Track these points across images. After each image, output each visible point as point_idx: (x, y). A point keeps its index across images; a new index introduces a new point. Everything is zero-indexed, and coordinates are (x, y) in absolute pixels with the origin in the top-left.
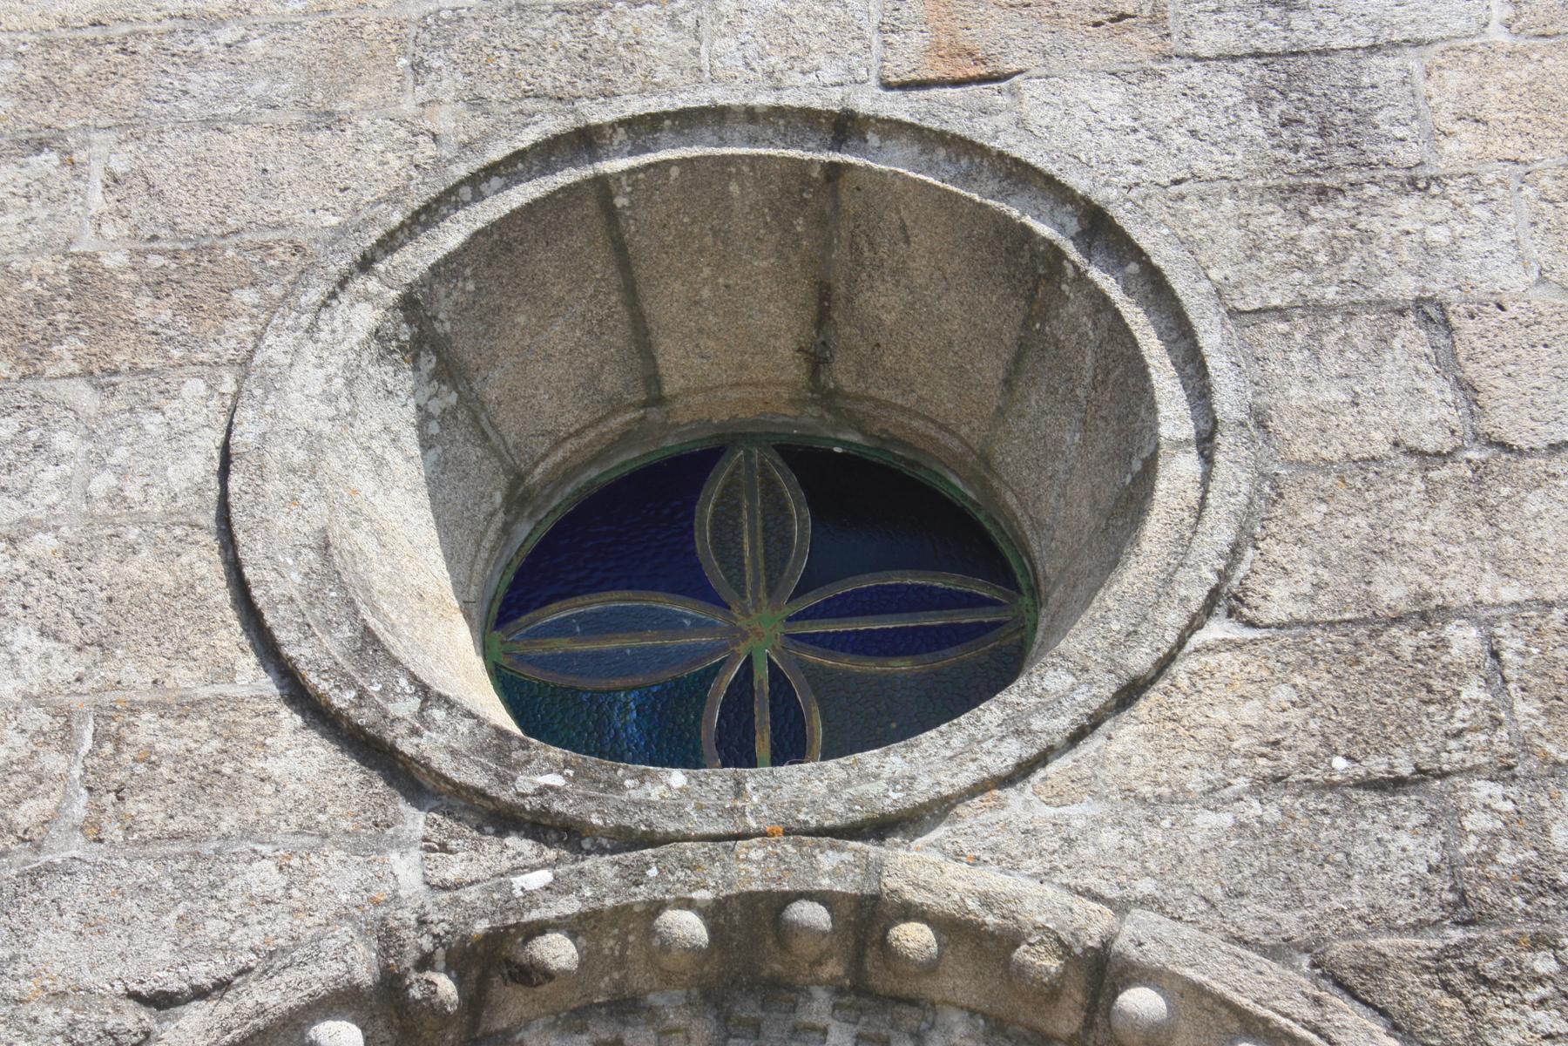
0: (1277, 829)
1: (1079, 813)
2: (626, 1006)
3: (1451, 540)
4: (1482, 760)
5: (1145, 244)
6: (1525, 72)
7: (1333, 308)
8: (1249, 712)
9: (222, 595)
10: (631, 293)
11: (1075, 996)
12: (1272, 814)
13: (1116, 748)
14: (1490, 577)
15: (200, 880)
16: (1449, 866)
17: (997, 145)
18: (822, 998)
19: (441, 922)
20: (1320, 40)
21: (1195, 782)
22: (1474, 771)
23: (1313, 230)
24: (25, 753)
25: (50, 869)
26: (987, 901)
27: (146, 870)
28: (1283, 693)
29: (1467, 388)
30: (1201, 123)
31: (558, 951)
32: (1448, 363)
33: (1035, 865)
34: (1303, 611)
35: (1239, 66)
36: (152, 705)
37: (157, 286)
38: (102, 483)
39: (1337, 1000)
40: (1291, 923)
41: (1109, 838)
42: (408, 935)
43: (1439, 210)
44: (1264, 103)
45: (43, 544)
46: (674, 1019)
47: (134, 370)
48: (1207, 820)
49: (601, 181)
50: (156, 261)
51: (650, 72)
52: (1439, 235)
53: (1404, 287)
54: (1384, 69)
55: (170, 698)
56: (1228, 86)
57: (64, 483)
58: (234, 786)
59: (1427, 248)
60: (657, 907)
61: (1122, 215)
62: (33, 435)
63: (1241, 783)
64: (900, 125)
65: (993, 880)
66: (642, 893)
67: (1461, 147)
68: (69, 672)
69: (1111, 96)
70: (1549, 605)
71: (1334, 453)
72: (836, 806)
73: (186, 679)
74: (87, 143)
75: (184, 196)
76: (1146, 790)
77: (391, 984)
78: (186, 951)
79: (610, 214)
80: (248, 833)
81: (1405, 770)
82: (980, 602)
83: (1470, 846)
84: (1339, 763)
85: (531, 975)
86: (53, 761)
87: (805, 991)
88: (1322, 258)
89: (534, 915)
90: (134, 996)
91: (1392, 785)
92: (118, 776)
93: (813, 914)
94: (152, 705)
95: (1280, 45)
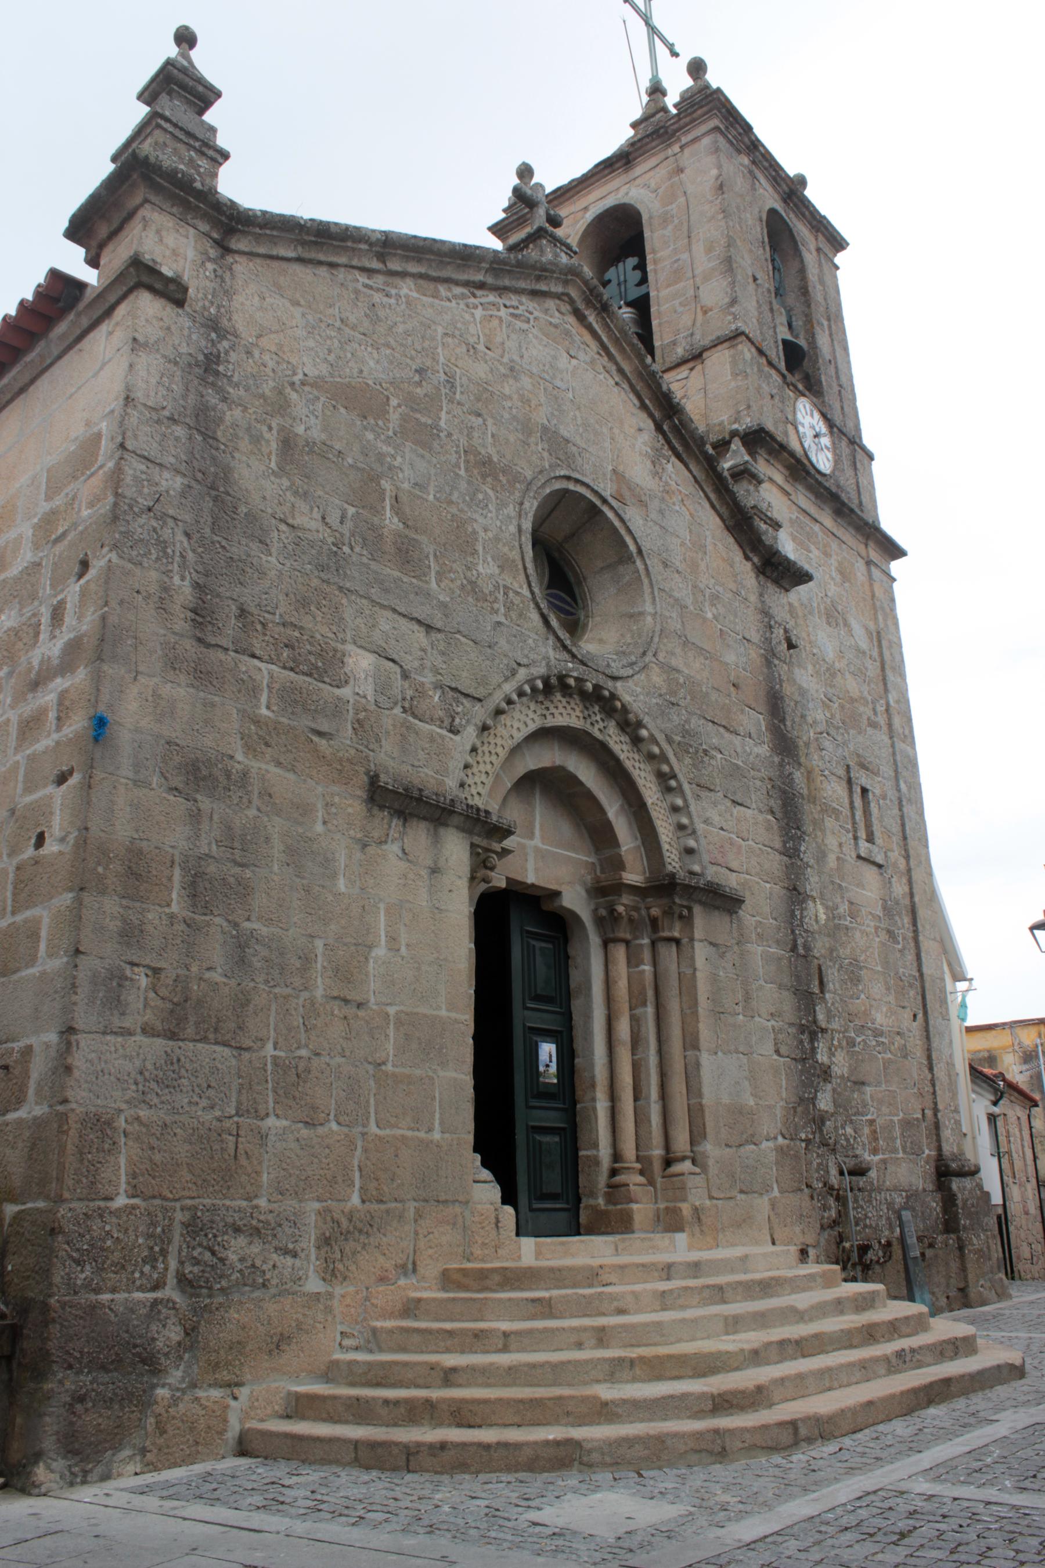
9: (520, 566)
31: (571, 682)
41: (642, 697)
45: (490, 534)
57: (492, 518)
60: (587, 680)
66: (585, 677)
73: (516, 586)
77: (549, 677)
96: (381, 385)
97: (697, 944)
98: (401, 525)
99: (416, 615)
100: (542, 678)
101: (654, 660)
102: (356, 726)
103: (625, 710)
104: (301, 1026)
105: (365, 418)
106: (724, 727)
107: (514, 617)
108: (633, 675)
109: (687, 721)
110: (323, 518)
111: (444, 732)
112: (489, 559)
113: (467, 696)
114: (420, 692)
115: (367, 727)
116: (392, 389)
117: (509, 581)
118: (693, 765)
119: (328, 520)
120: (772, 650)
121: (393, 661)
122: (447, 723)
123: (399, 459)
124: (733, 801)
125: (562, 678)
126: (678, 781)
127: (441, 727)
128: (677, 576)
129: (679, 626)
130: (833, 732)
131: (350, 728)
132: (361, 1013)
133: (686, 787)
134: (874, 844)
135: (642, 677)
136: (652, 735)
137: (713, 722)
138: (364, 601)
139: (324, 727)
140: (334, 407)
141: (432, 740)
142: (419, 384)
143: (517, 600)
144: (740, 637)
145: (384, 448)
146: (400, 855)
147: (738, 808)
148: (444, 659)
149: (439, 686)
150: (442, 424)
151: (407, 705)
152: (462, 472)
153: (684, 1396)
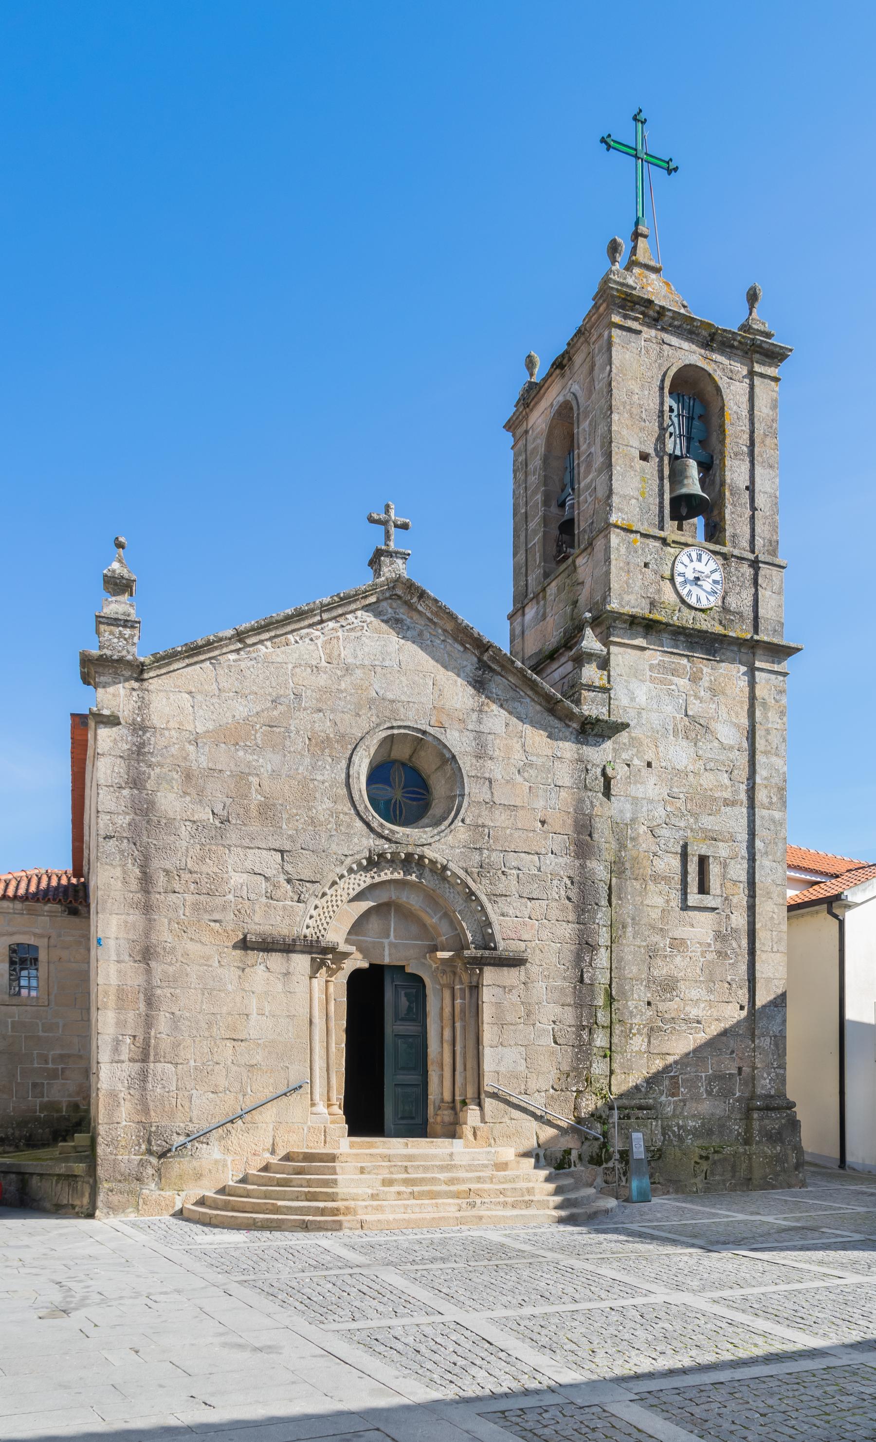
1: (444, 847)
19: (377, 850)
31: (389, 856)
32: (491, 788)
37: (338, 742)
38: (333, 775)
45: (327, 784)
48: (458, 851)
53: (487, 775)
54: (490, 737)
56: (471, 735)
65: (436, 855)
67: (497, 753)
68: (332, 805)
77: (370, 857)
78: (349, 849)
82: (424, 795)
86: (331, 819)
93: (417, 857)
98: (263, 799)
101: (461, 824)
102: (236, 912)
107: (343, 829)
109: (489, 857)
112: (326, 799)
114: (276, 886)
117: (339, 807)
120: (586, 786)
122: (296, 898)
124: (529, 899)
125: (381, 856)
128: (489, 762)
129: (489, 796)
130: (674, 821)
133: (484, 898)
134: (708, 894)
135: (450, 838)
136: (453, 873)
138: (239, 849)
139: (217, 916)
141: (284, 908)
144: (553, 786)
147: (533, 902)
149: (289, 881)
151: (268, 895)
152: (306, 753)
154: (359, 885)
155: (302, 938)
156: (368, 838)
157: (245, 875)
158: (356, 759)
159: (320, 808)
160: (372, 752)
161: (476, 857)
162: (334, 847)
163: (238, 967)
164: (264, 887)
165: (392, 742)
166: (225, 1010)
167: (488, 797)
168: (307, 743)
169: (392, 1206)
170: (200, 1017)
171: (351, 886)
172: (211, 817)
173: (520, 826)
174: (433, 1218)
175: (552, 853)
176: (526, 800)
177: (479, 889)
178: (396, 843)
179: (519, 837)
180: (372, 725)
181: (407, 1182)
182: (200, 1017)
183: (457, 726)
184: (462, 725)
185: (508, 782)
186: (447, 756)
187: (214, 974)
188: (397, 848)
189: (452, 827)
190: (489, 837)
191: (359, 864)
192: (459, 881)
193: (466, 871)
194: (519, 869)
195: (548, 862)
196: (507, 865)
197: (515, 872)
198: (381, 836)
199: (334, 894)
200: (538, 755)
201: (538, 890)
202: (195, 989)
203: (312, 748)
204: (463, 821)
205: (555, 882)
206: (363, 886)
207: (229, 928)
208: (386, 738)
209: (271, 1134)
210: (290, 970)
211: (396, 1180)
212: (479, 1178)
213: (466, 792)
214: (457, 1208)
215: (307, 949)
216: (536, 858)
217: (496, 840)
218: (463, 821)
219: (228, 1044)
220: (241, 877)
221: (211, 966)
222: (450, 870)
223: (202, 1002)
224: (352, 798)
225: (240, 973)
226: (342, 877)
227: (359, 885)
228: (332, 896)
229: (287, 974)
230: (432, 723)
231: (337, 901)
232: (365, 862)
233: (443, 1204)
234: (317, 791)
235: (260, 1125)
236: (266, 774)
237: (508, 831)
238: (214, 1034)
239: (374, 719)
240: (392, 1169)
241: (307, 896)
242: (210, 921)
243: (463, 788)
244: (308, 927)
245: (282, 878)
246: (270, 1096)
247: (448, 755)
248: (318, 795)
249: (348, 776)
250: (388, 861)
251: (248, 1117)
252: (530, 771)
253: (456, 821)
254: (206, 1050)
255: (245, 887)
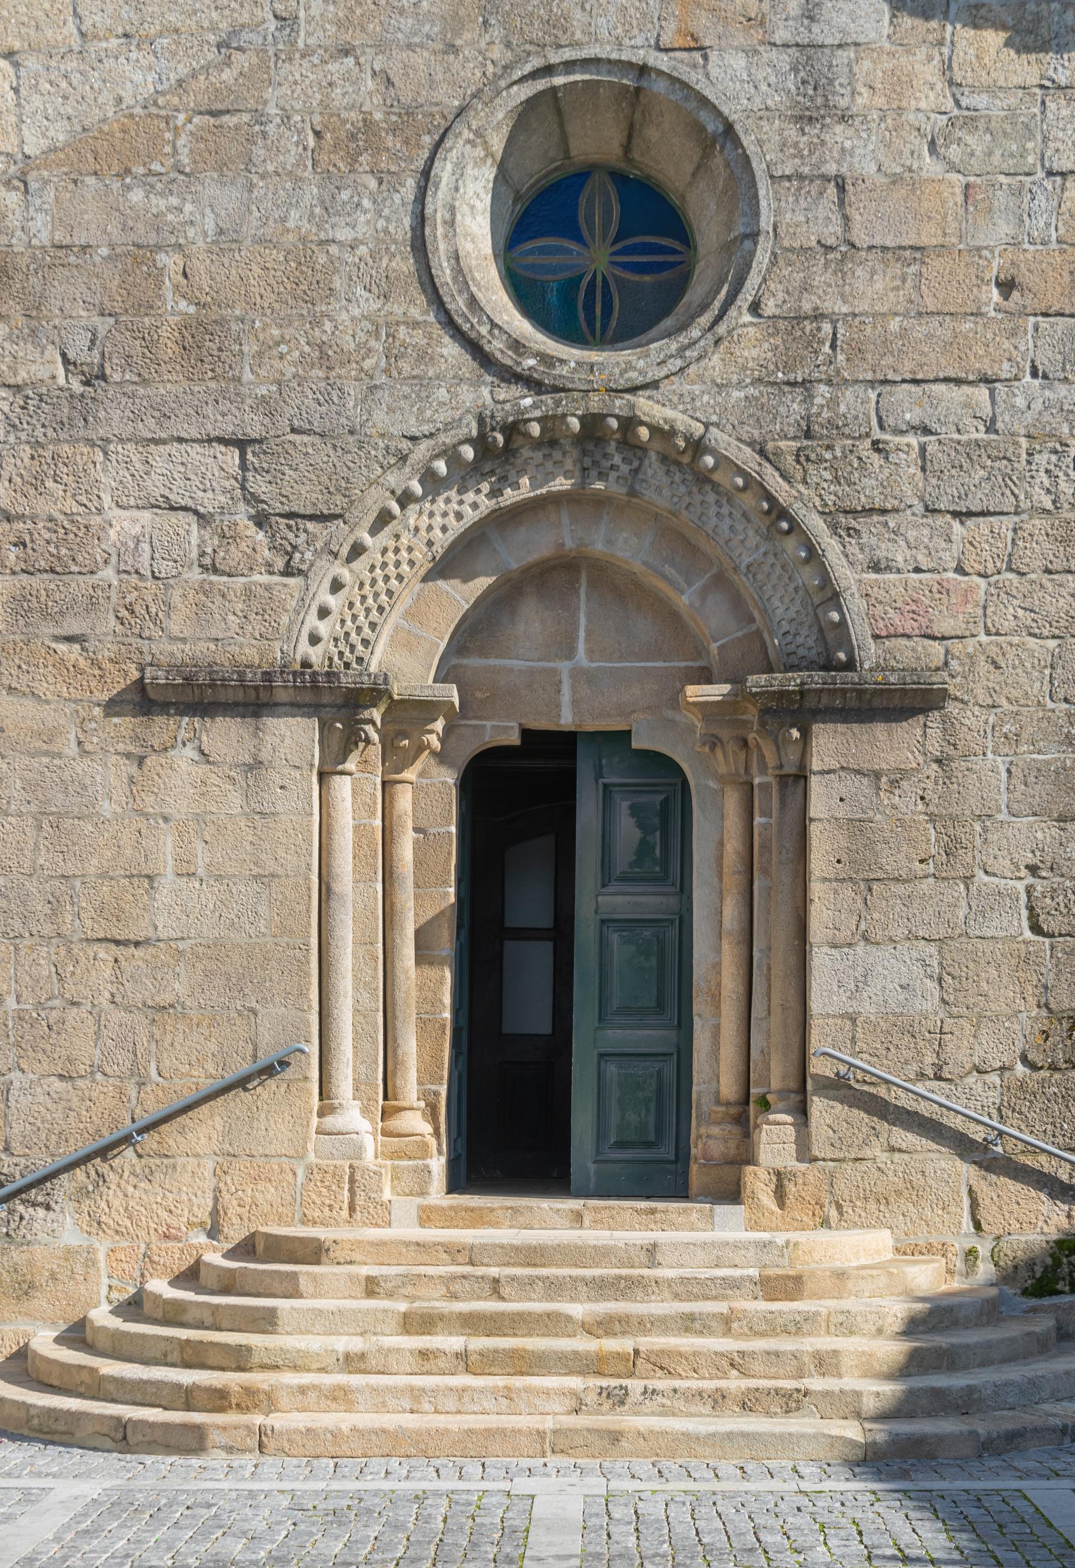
0: (756, 399)
1: (697, 388)
2: (553, 443)
3: (830, 286)
4: (823, 377)
5: (745, 144)
6: (888, 65)
7: (806, 177)
8: (755, 353)
10: (562, 125)
11: (690, 453)
12: (757, 393)
13: (711, 364)
14: (839, 302)
15: (423, 394)
16: (808, 418)
17: (698, 87)
18: (613, 444)
20: (820, 40)
21: (735, 378)
22: (820, 381)
23: (805, 138)
24: (364, 340)
25: (376, 387)
26: (666, 421)
27: (406, 389)
28: (766, 346)
29: (846, 218)
30: (772, 79)
31: (535, 429)
33: (681, 407)
34: (777, 312)
35: (789, 51)
36: (404, 323)
38: (381, 223)
39: (768, 465)
40: (756, 434)
41: (706, 398)
42: (488, 420)
43: (850, 132)
44: (795, 69)
45: (363, 250)
46: (567, 448)
47: (389, 172)
49: (553, 90)
50: (394, 118)
51: (573, 34)
52: (848, 144)
53: (831, 169)
55: (410, 320)
56: (784, 60)
57: (368, 222)
58: (432, 359)
59: (843, 149)
60: (564, 416)
61: (738, 127)
62: (356, 199)
63: (748, 381)
64: (663, 73)
68: (376, 307)
69: (738, 62)
70: (855, 315)
71: (796, 245)
72: (622, 381)
74: (364, 53)
75: (402, 86)
76: (719, 381)
78: (420, 421)
79: (556, 99)
80: (438, 378)
81: (800, 379)
83: (814, 410)
84: (780, 375)
85: (527, 435)
86: (372, 343)
87: (608, 442)
88: (806, 152)
89: (527, 416)
90: (404, 436)
91: (793, 384)
92: (395, 351)
94: (404, 323)
95: (806, 41)
96: (156, 104)
97: (814, 780)
98: (192, 309)
99: (214, 434)
100: (468, 441)
101: (747, 318)
102: (124, 613)
103: (663, 433)
104: (54, 976)
105: (128, 171)
106: (947, 380)
108: (682, 369)
110: (64, 355)
111: (276, 579)
112: (360, 291)
113: (311, 518)
115: (137, 608)
116: (176, 100)
118: (837, 480)
119: (71, 355)
121: (185, 509)
122: (280, 563)
123: (188, 207)
125: (513, 429)
126: (791, 520)
127: (271, 573)
128: (839, 129)
131: (111, 616)
132: (139, 953)
133: (816, 525)
136: (723, 461)
137: (915, 382)
139: (73, 626)
140: (75, 182)
141: (248, 593)
142: (228, 62)
143: (418, 338)
144: (1040, 174)
145: (162, 203)
146: (196, 758)
147: (970, 522)
148: (268, 477)
149: (261, 520)
150: (271, 109)
151: (207, 561)
152: (308, 173)
153: (159, 1384)
154: (459, 516)
155: (297, 667)
156: (477, 384)
157: (146, 515)
158: (444, 171)
159: (344, 316)
160: (498, 143)
161: (794, 407)
162: (380, 416)
163: (128, 755)
164: (194, 540)
165: (559, 112)
166: (92, 866)
167: (832, 232)
168: (311, 141)
169: (374, 1390)
170: (32, 886)
171: (438, 520)
172: (61, 371)
173: (931, 304)
174: (470, 1432)
175: (1034, 374)
176: (952, 226)
177: (800, 497)
178: (556, 389)
179: (929, 336)
180: (490, 69)
181: (471, 1323)
182: (32, 886)
183: (740, 40)
184: (758, 34)
185: (895, 180)
186: (710, 128)
187: (66, 776)
188: (557, 404)
189: (721, 329)
190: (833, 346)
191: (451, 455)
192: (740, 481)
193: (762, 452)
194: (927, 431)
195: (1020, 402)
196: (891, 421)
197: (913, 440)
198: (510, 376)
199: (391, 544)
200: (992, 90)
201: (987, 487)
202: (20, 815)
203: (324, 158)
204: (755, 308)
205: (1042, 459)
206: (471, 516)
207: (106, 653)
208: (531, 103)
209: (210, 1183)
210: (265, 755)
211: (441, 1317)
212: (691, 1317)
213: (766, 222)
214: (570, 1403)
215: (308, 698)
216: (982, 393)
217: (857, 352)
218: (755, 308)
219: (102, 955)
220: (134, 521)
221: (60, 755)
222: (713, 452)
223: (36, 848)
224: (431, 277)
225: (134, 770)
226: (405, 499)
227: (459, 516)
228: (385, 551)
229: (255, 765)
230: (666, 40)
231: (397, 564)
232: (468, 452)
233: (528, 1390)
234: (336, 271)
235: (180, 1161)
236: (201, 244)
237: (894, 325)
238: (66, 929)
239: (497, 52)
240: (456, 1287)
241: (308, 555)
242: (57, 638)
243: (757, 214)
244: (314, 640)
245: (242, 515)
246: (208, 1085)
247: (712, 126)
248: (337, 283)
249: (420, 220)
250: (538, 444)
251: (149, 1141)
252: (969, 139)
253: (733, 312)
254: (46, 970)
255: (146, 547)
